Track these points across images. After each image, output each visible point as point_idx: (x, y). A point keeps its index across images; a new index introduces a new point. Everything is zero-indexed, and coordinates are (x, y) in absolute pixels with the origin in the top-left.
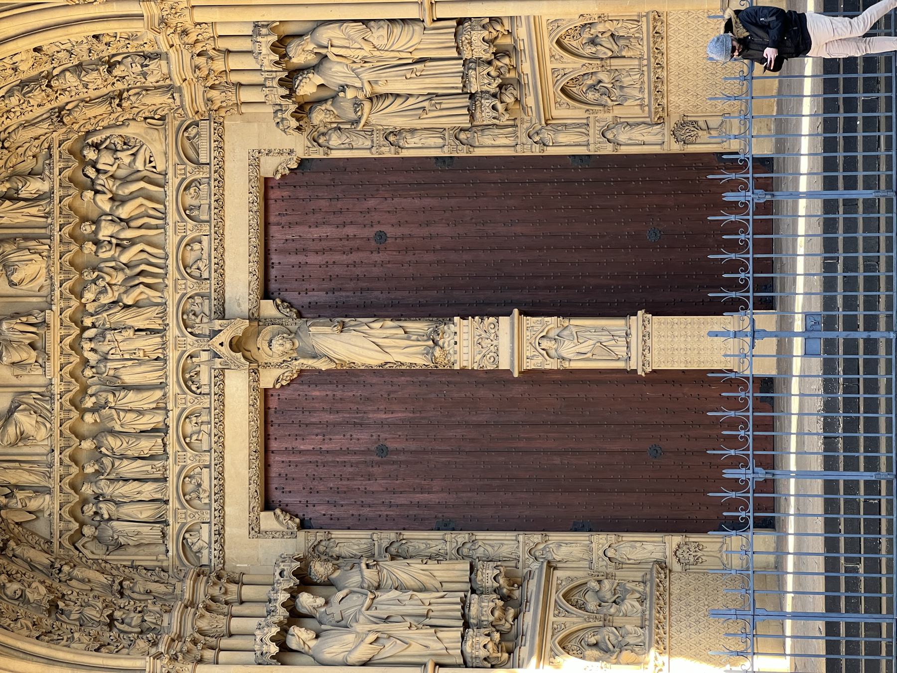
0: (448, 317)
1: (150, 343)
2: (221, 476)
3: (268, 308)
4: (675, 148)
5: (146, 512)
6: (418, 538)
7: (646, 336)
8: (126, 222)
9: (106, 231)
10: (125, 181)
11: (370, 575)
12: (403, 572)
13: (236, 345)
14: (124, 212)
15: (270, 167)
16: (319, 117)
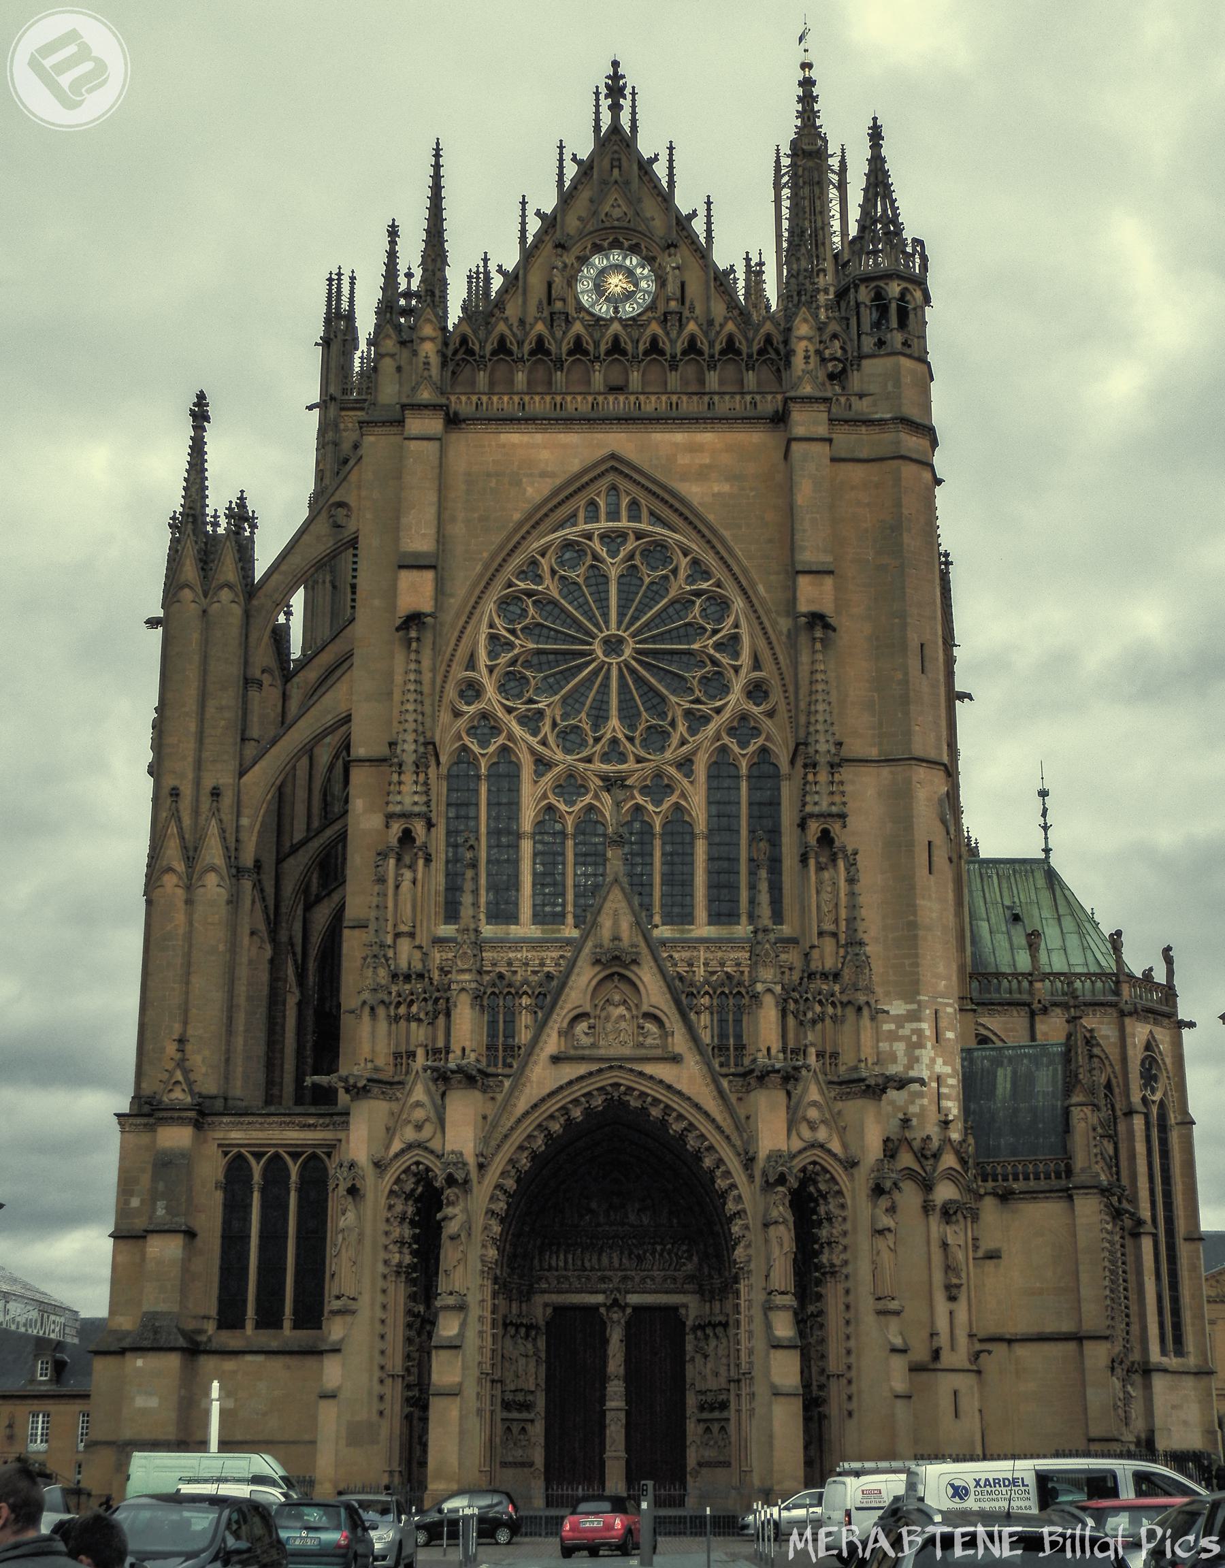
0: (626, 1381)
1: (617, 1265)
2: (567, 1292)
3: (629, 1310)
4: (688, 1469)
5: (554, 1263)
6: (543, 1368)
7: (617, 1458)
8: (661, 1255)
9: (659, 1248)
10: (676, 1254)
11: (531, 1353)
12: (532, 1364)
13: (616, 1301)
14: (665, 1254)
15: (683, 1311)
16: (699, 1333)
